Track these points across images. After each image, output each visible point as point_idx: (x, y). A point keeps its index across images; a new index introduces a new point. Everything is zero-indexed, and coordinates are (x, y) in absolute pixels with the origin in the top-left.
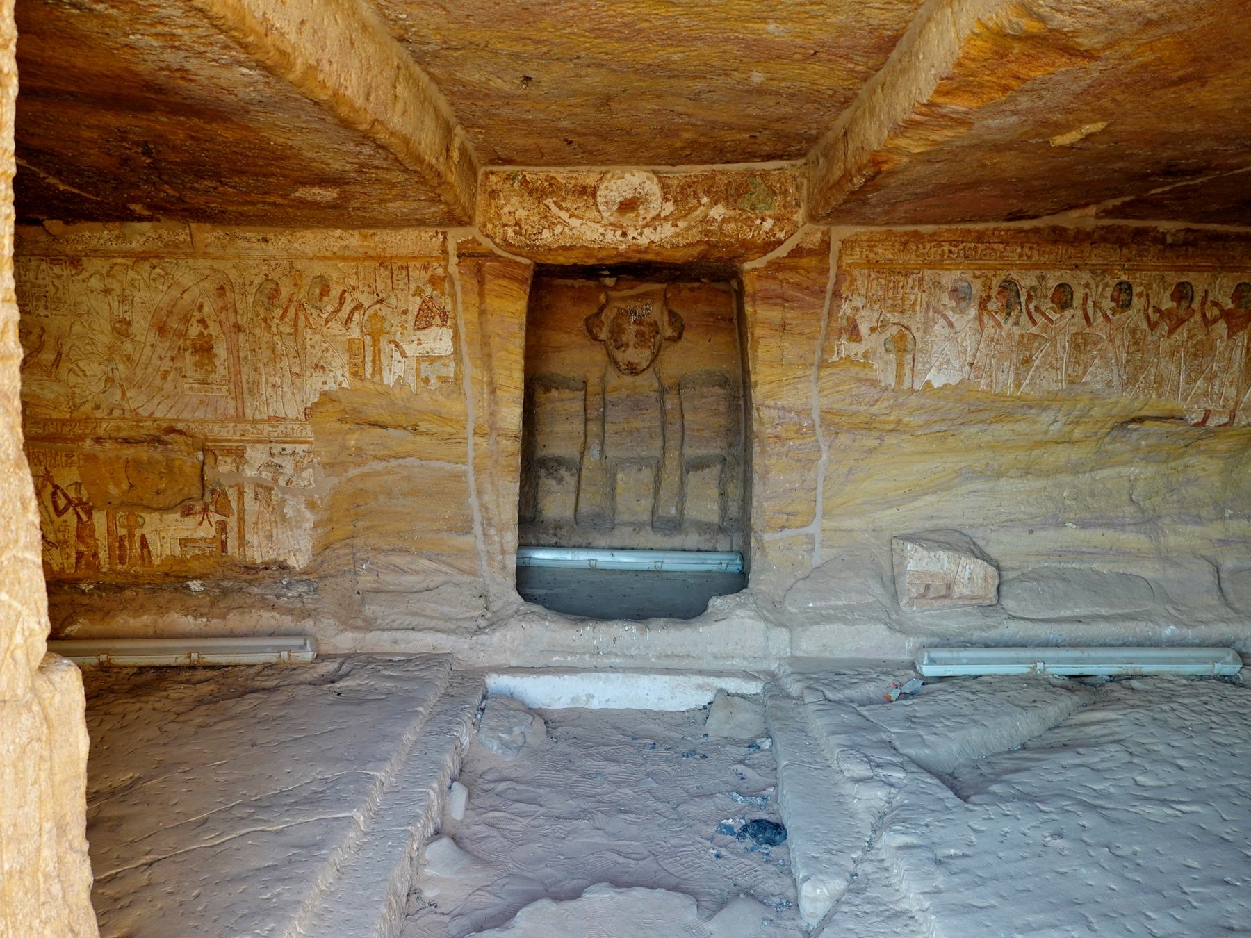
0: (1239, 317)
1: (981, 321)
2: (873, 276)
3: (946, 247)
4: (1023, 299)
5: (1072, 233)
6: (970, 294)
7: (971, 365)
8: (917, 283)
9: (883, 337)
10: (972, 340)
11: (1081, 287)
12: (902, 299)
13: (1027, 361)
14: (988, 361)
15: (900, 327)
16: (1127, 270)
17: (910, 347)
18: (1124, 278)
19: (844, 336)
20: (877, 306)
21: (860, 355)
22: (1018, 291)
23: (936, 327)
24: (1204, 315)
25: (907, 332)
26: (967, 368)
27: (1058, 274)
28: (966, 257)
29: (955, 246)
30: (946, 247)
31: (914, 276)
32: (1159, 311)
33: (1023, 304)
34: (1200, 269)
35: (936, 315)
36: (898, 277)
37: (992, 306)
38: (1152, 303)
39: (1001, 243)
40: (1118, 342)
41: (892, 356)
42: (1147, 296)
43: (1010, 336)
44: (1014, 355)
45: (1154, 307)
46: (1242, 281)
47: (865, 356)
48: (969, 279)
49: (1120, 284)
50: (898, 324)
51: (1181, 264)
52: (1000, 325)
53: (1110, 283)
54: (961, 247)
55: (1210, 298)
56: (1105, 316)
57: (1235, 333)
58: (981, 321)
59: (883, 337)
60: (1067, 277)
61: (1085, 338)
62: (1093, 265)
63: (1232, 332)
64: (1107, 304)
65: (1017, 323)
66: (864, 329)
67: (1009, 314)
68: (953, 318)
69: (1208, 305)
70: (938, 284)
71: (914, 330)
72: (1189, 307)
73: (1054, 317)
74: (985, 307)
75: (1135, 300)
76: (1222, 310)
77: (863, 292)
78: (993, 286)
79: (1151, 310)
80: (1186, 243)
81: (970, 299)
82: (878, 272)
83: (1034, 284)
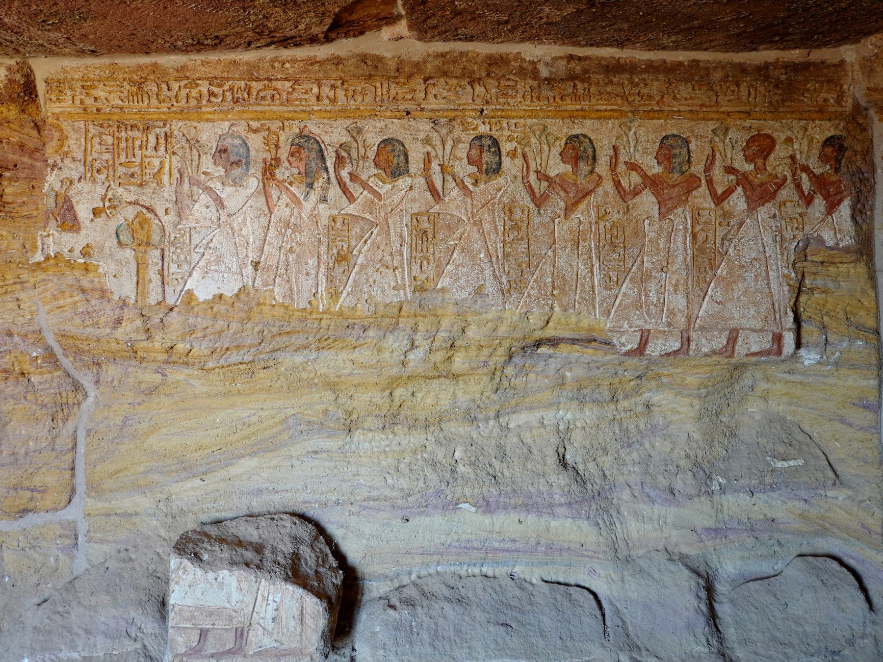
0: (673, 186)
1: (267, 197)
2: (93, 130)
3: (204, 87)
4: (330, 163)
5: (392, 65)
6: (247, 157)
7: (256, 265)
8: (162, 141)
9: (113, 224)
10: (256, 226)
11: (419, 144)
12: (141, 164)
13: (342, 258)
14: (283, 258)
15: (139, 208)
16: (486, 117)
17: (155, 238)
18: (484, 129)
19: (53, 223)
20: (103, 176)
21: (77, 252)
22: (321, 150)
23: (197, 206)
24: (618, 184)
25: (149, 215)
26: (250, 269)
27: (380, 124)
28: (236, 101)
29: (220, 86)
30: (204, 87)
31: (158, 130)
32: (547, 178)
33: (331, 170)
34: (601, 116)
35: (195, 188)
36: (136, 134)
37: (281, 173)
38: (533, 165)
39: (286, 79)
40: (487, 226)
41: (128, 253)
42: (524, 156)
43: (314, 217)
44: (323, 248)
45: (537, 172)
46: (670, 132)
47: (85, 253)
48: (244, 134)
49: (480, 137)
50: (136, 203)
51: (570, 107)
52: (298, 202)
53: (464, 137)
54: (226, 87)
55: (623, 158)
56: (462, 185)
57: (670, 210)
58: (267, 197)
59: (113, 224)
60: (395, 128)
61: (433, 220)
62: (432, 110)
63: (665, 208)
64: (463, 169)
65: (324, 200)
66: (83, 212)
67: (311, 186)
68: (225, 193)
69: (621, 168)
70: (194, 143)
71: (161, 212)
72: (592, 172)
73: (384, 189)
74: (272, 175)
75: (506, 162)
76: (644, 176)
77: (80, 155)
78: (280, 144)
79: (533, 177)
80: (572, 77)
81: (247, 164)
82: (101, 126)
83: (344, 140)
